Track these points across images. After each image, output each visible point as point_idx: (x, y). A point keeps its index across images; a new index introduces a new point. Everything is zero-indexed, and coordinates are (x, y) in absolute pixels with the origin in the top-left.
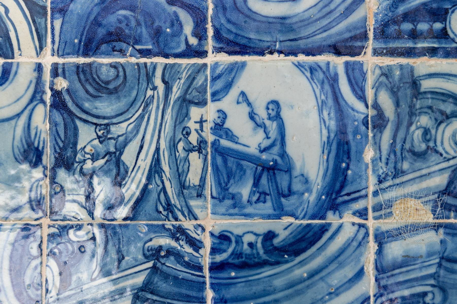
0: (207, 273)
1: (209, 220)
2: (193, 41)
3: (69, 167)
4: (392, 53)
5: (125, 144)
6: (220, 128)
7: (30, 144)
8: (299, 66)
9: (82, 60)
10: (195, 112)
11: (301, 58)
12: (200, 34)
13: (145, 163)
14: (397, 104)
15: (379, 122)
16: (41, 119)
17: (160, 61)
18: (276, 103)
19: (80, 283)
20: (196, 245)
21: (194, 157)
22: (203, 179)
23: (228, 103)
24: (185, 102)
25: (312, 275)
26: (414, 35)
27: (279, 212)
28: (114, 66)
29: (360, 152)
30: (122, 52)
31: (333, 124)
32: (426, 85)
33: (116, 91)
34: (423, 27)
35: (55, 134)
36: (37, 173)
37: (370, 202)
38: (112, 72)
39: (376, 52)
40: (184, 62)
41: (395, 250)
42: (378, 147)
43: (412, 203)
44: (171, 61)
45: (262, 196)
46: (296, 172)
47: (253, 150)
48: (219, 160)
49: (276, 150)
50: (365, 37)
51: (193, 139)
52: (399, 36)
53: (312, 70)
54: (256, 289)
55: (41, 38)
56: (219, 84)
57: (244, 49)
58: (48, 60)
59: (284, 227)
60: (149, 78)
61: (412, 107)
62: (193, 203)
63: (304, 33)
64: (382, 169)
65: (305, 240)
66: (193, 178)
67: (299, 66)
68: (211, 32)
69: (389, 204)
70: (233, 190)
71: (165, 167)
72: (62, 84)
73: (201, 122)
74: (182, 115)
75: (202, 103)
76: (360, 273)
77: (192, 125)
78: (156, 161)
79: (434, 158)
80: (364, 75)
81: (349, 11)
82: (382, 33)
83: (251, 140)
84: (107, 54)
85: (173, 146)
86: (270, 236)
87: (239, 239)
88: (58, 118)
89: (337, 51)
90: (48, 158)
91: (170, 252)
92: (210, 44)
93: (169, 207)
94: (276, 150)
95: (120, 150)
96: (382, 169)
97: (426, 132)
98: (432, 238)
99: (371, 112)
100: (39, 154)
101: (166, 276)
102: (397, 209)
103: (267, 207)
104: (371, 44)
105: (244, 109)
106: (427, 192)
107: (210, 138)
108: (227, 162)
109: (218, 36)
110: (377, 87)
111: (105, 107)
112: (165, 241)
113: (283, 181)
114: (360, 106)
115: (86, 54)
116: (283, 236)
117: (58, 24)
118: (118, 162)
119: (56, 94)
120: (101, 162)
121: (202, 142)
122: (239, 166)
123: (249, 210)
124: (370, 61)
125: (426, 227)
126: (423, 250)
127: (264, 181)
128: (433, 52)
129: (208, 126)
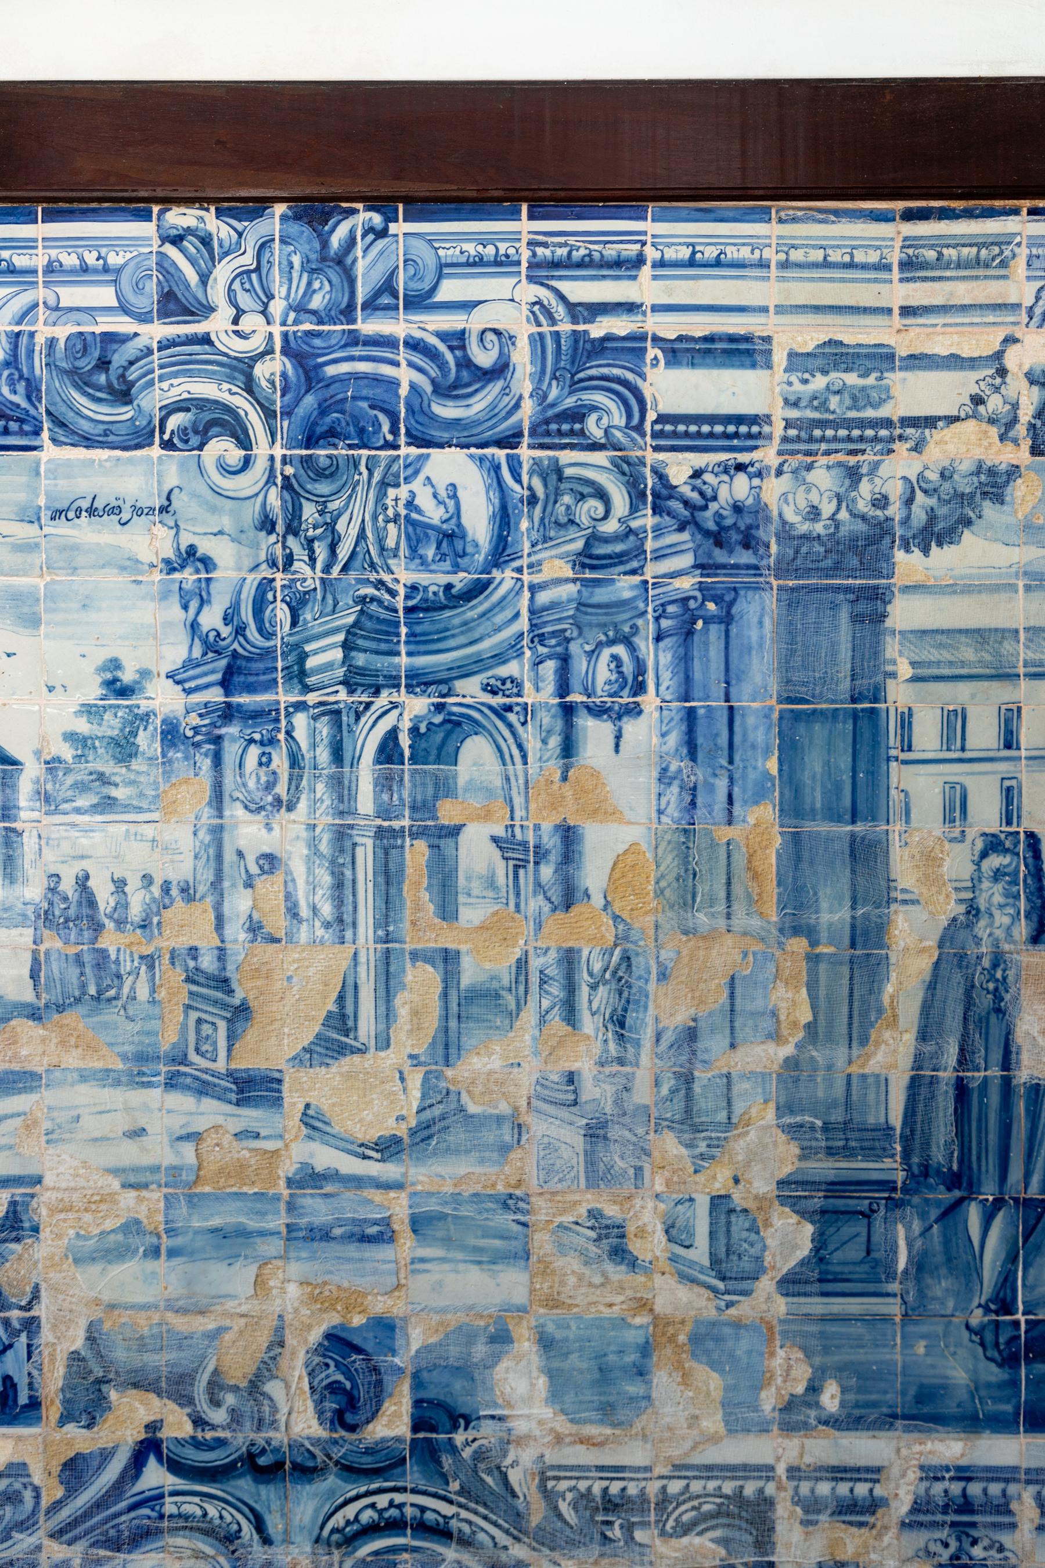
0: (401, 613)
1: (403, 574)
2: (390, 437)
3: (296, 534)
4: (542, 446)
5: (339, 516)
6: (410, 504)
7: (267, 516)
8: (471, 456)
9: (304, 452)
10: (392, 492)
11: (473, 450)
12: (394, 430)
13: (354, 531)
14: (546, 486)
15: (533, 500)
16: (274, 498)
17: (365, 452)
18: (453, 485)
19: (305, 622)
20: (393, 593)
21: (391, 526)
22: (398, 544)
23: (416, 485)
24: (384, 485)
25: (483, 615)
26: (560, 433)
27: (456, 568)
28: (329, 457)
29: (518, 524)
30: (335, 446)
31: (497, 501)
32: (569, 472)
33: (332, 475)
34: (565, 427)
35: (285, 508)
36: (273, 538)
37: (525, 562)
38: (328, 462)
39: (531, 447)
40: (382, 453)
41: (544, 598)
42: (531, 518)
43: (558, 562)
44: (373, 452)
45: (443, 557)
46: (469, 538)
47: (436, 521)
48: (410, 529)
49: (454, 521)
50: (519, 434)
51: (390, 513)
52: (548, 433)
53: (482, 459)
54: (441, 626)
55: (273, 435)
56: (410, 471)
57: (428, 444)
58: (279, 452)
59: (460, 580)
60: (356, 466)
61: (557, 488)
62: (390, 562)
63: (475, 431)
64: (535, 535)
65: (478, 589)
66: (390, 543)
67: (471, 456)
68: (403, 431)
69: (540, 563)
70: (421, 552)
71: (369, 534)
72: (289, 470)
73: (396, 500)
74: (381, 495)
75: (397, 485)
76: (517, 615)
77: (389, 502)
78: (362, 530)
79: (574, 528)
80: (520, 464)
81: (510, 413)
82: (533, 433)
83: (433, 513)
84: (324, 448)
85: (375, 517)
86: (449, 587)
87: (425, 589)
88: (287, 497)
89: (500, 443)
90: (280, 528)
91: (373, 599)
92: (403, 439)
93: (373, 566)
94: (454, 521)
95: (335, 521)
96: (535, 535)
97: (568, 507)
98: (572, 589)
99: (526, 493)
100: (273, 524)
101: (371, 617)
102: (545, 567)
103: (447, 565)
104: (526, 440)
105: (429, 490)
106: (568, 554)
107: (403, 512)
108: (416, 531)
109: (408, 433)
110: (531, 473)
111: (323, 488)
112: (370, 591)
113: (459, 545)
114: (517, 487)
115: (307, 448)
116: (459, 586)
117: (286, 424)
118: (333, 531)
119: (286, 478)
120: (319, 531)
121: (397, 515)
122: (427, 535)
123: (433, 567)
124: (525, 453)
125: (567, 580)
126: (564, 598)
127: (445, 544)
128: (572, 447)
129: (401, 503)
